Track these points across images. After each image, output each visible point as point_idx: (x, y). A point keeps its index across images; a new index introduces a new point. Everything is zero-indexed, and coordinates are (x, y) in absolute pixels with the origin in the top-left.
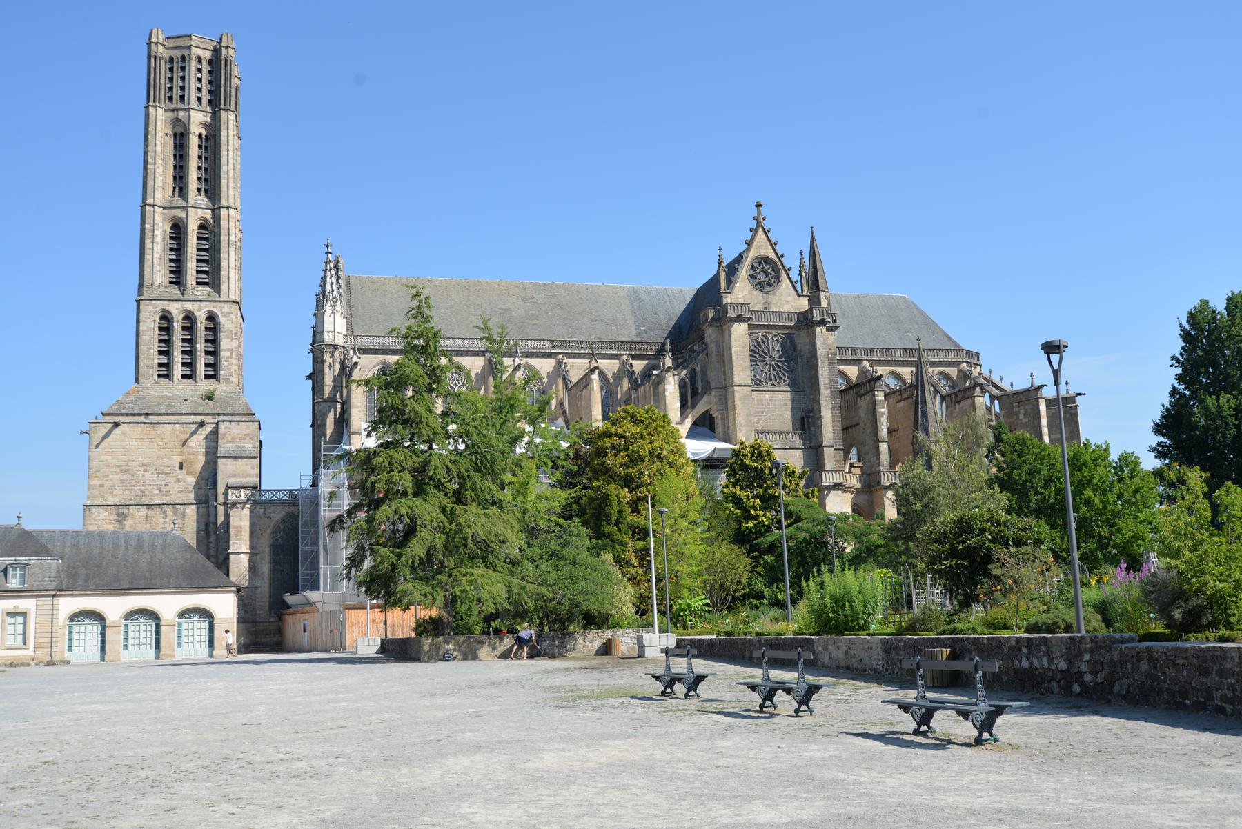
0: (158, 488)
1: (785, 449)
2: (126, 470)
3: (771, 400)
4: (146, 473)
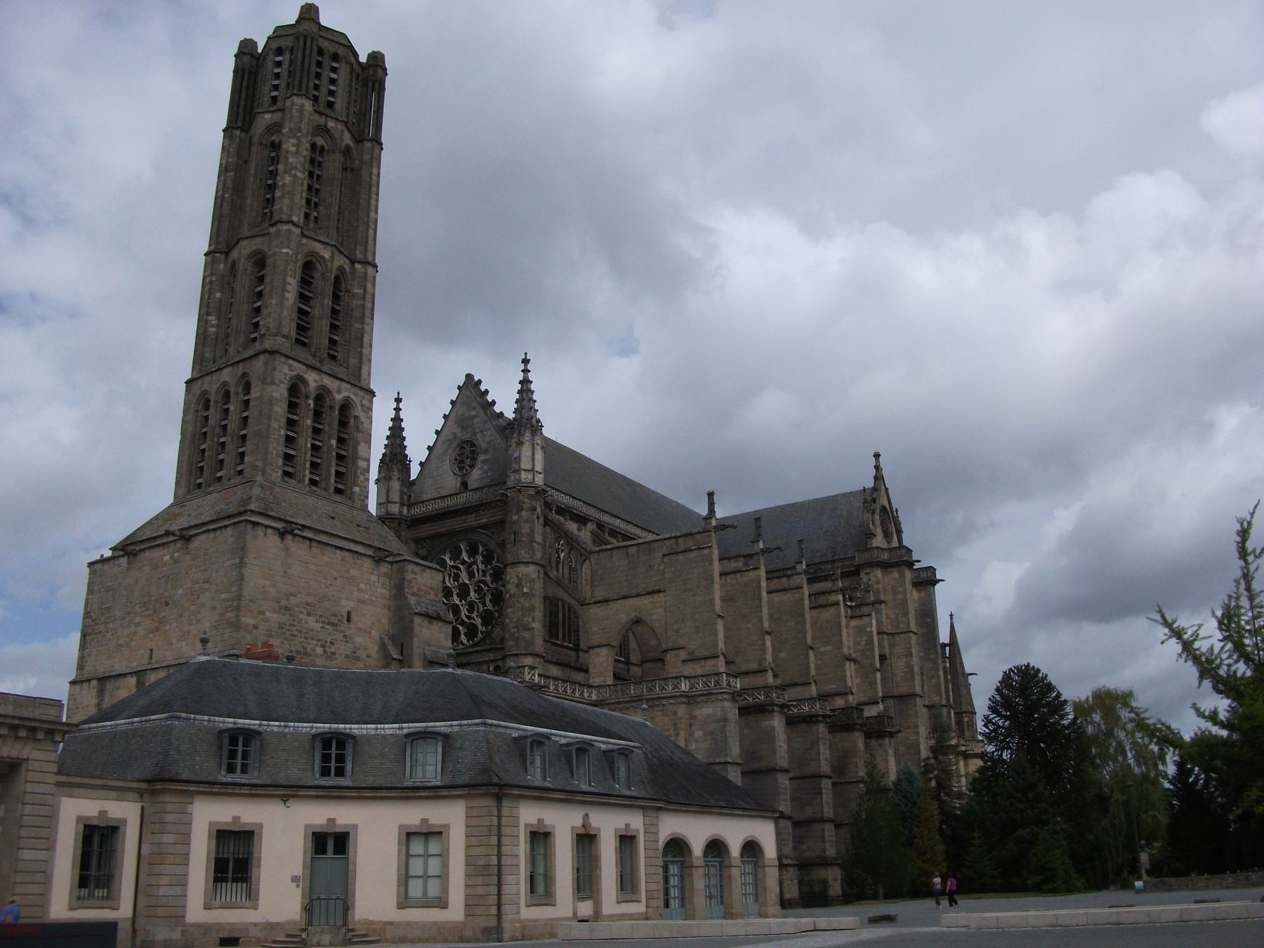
0: (323, 646)
2: (287, 609)
4: (311, 620)
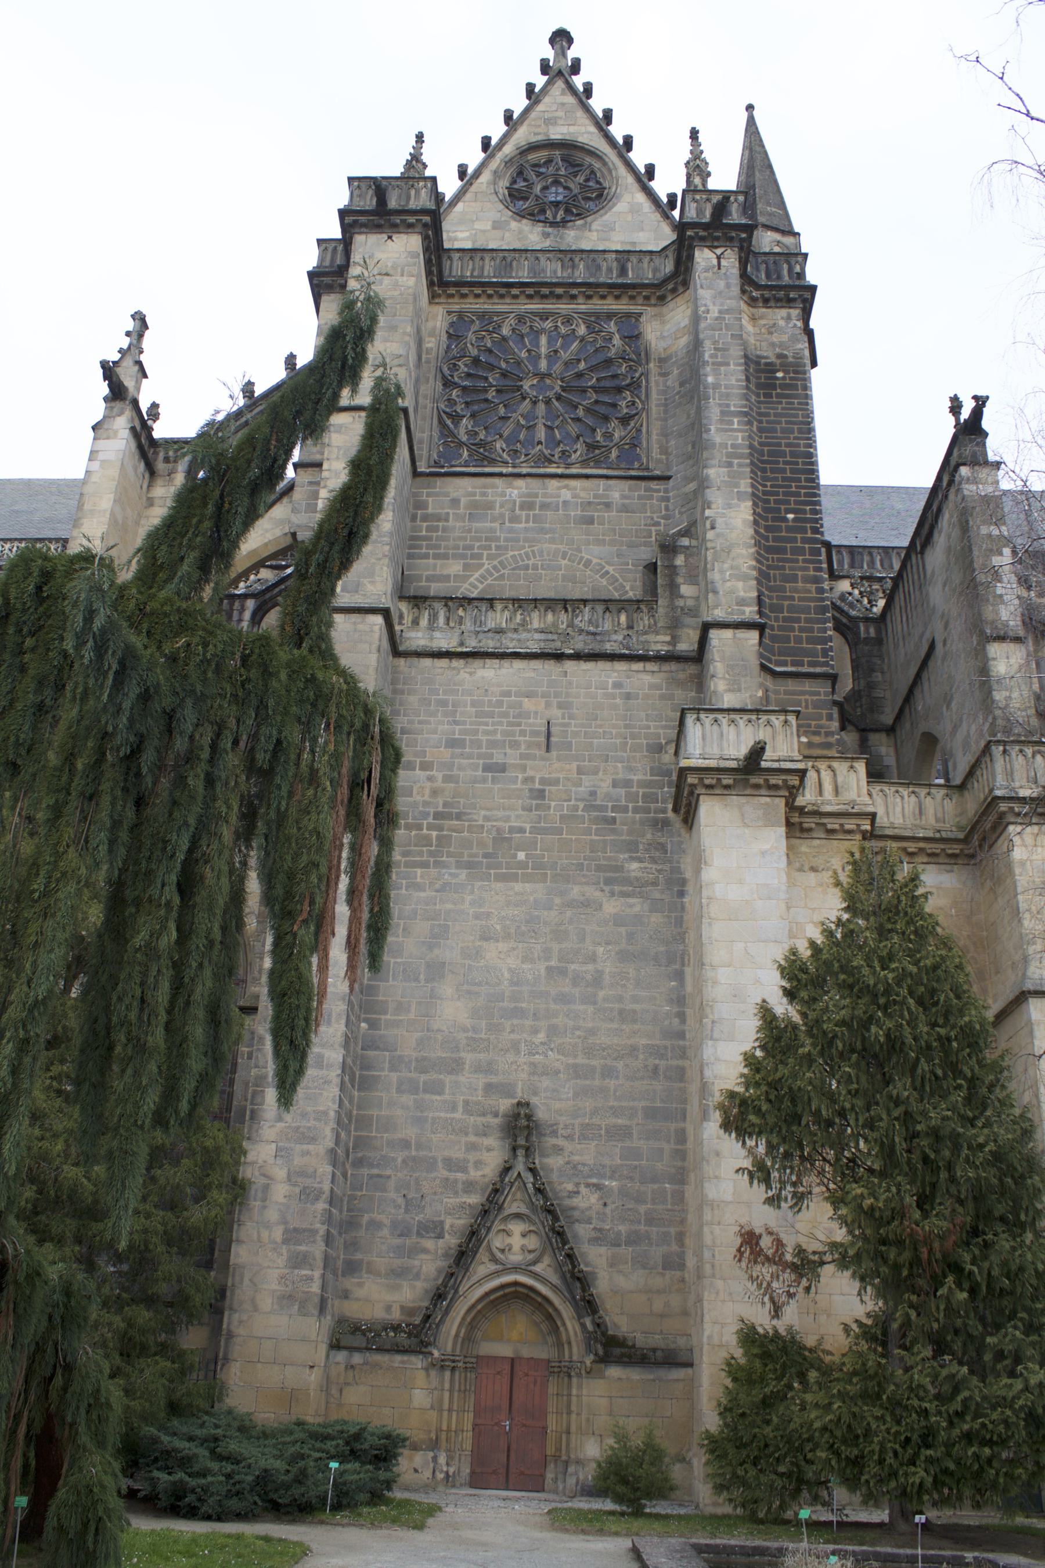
1: (559, 657)
3: (527, 506)
